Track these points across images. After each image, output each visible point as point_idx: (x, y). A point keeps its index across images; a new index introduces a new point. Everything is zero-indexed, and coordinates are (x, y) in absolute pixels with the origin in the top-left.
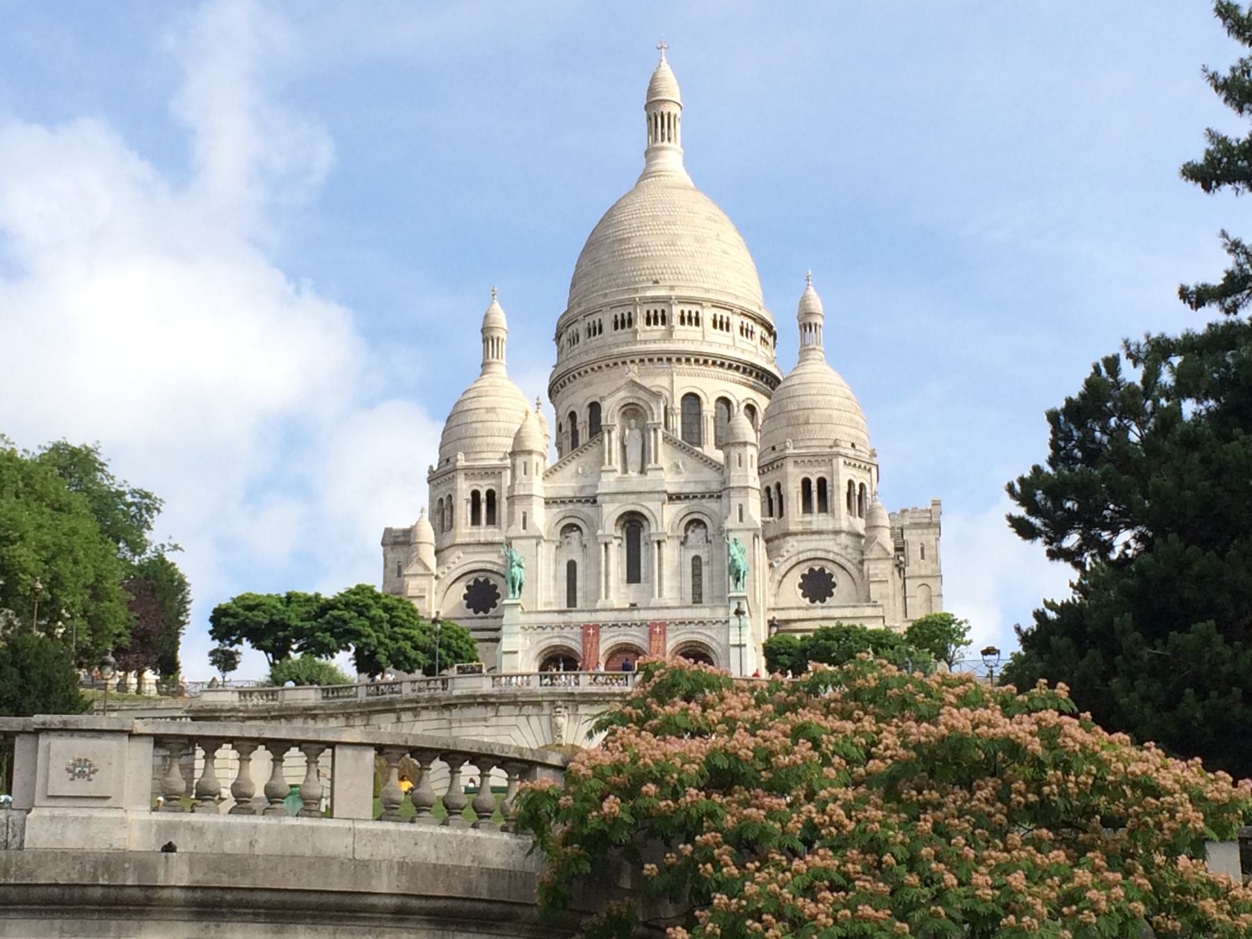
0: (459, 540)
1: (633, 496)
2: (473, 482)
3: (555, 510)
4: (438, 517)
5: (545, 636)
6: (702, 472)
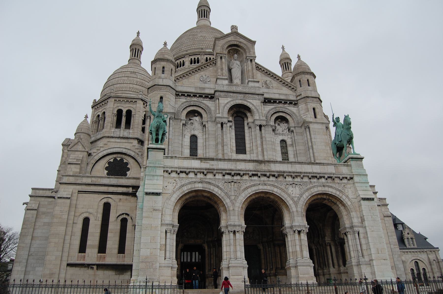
0: (107, 135)
1: (242, 95)
2: (119, 105)
3: (183, 100)
4: (95, 126)
5: (187, 181)
6: (282, 89)
